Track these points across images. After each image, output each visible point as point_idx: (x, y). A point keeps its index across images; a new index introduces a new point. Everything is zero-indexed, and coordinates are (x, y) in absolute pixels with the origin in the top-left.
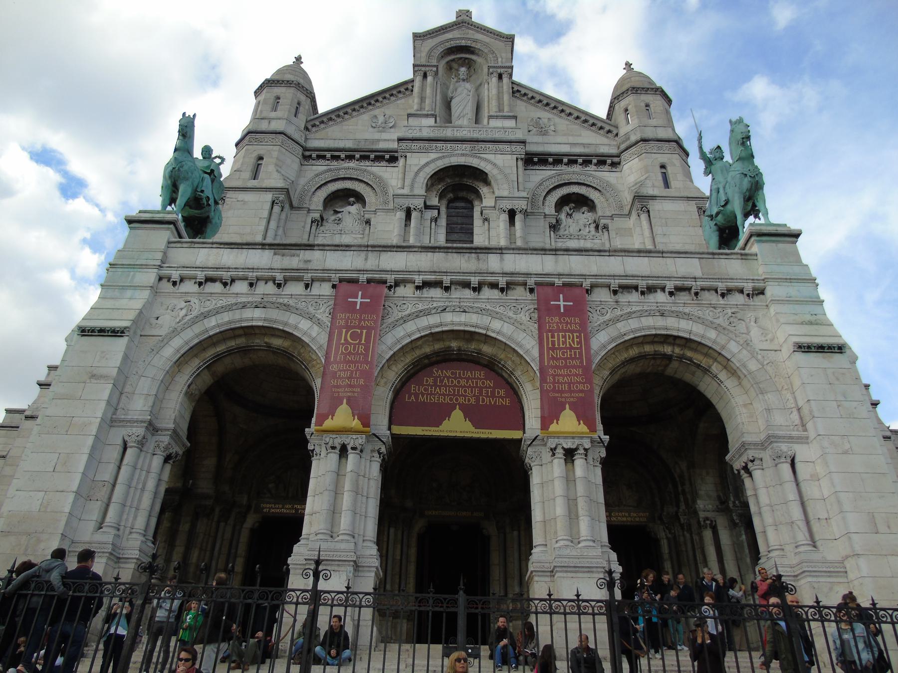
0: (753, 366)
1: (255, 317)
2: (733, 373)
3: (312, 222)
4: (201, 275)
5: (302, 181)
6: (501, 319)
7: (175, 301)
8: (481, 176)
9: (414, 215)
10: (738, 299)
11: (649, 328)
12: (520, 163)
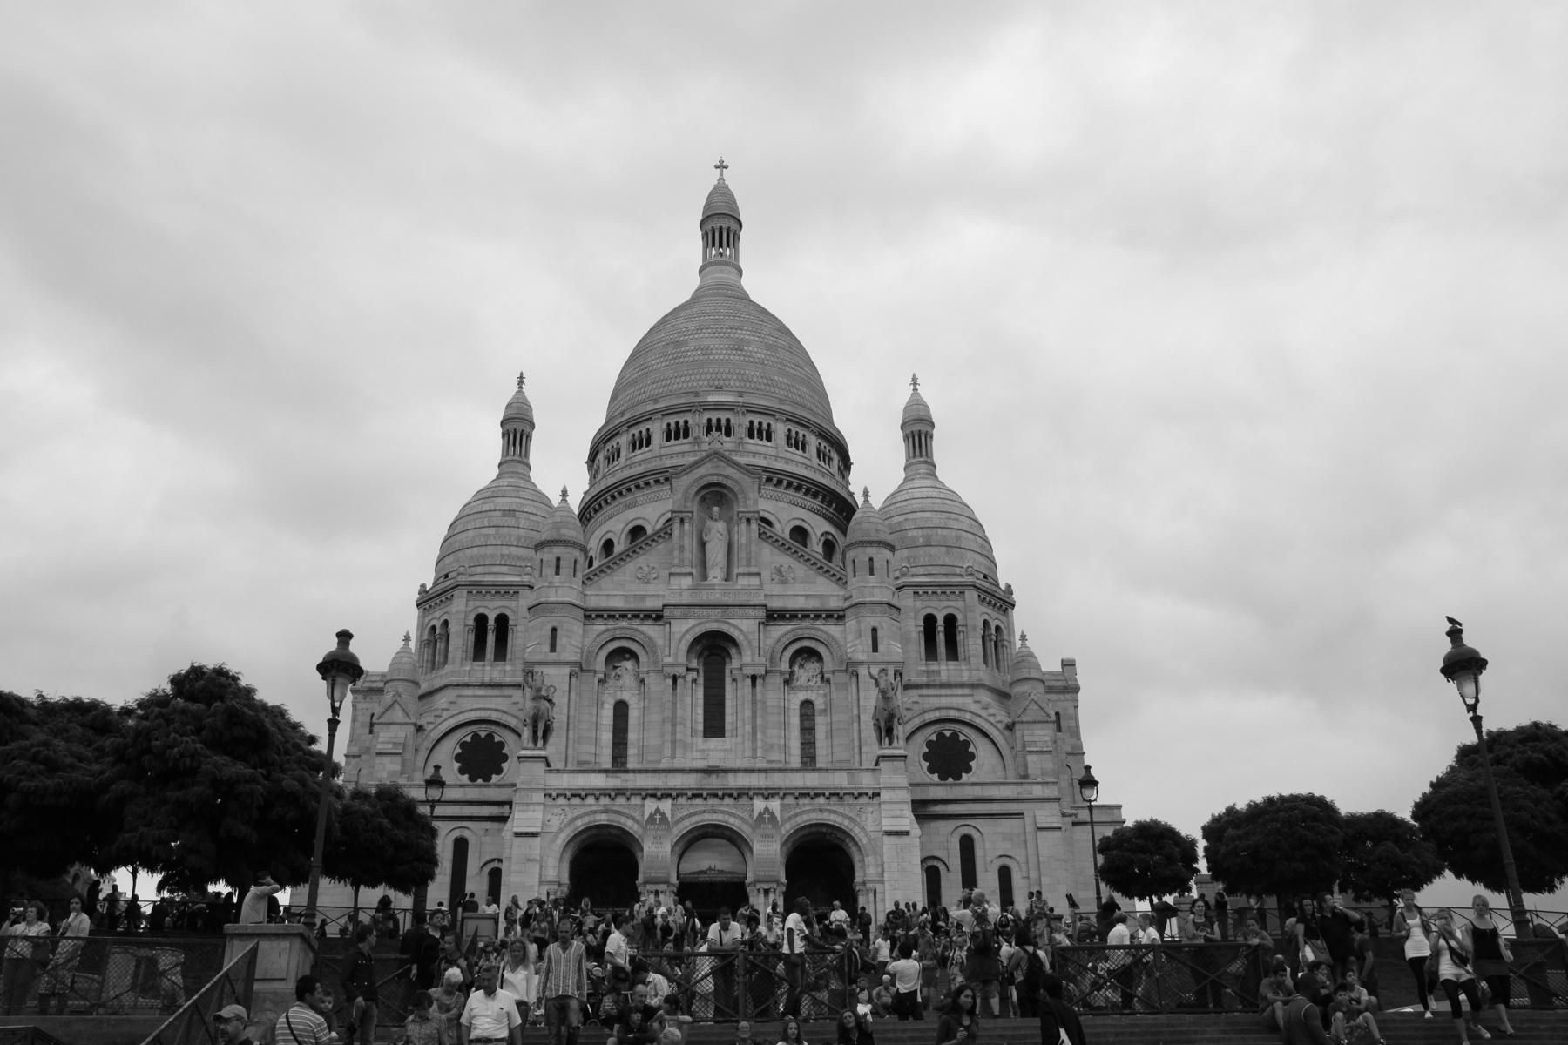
0: (865, 840)
1: (602, 819)
2: (856, 844)
3: (599, 682)
4: (569, 794)
5: (587, 642)
6: (735, 817)
7: (555, 811)
8: (732, 641)
9: (679, 681)
10: (864, 800)
11: (814, 820)
12: (761, 627)
